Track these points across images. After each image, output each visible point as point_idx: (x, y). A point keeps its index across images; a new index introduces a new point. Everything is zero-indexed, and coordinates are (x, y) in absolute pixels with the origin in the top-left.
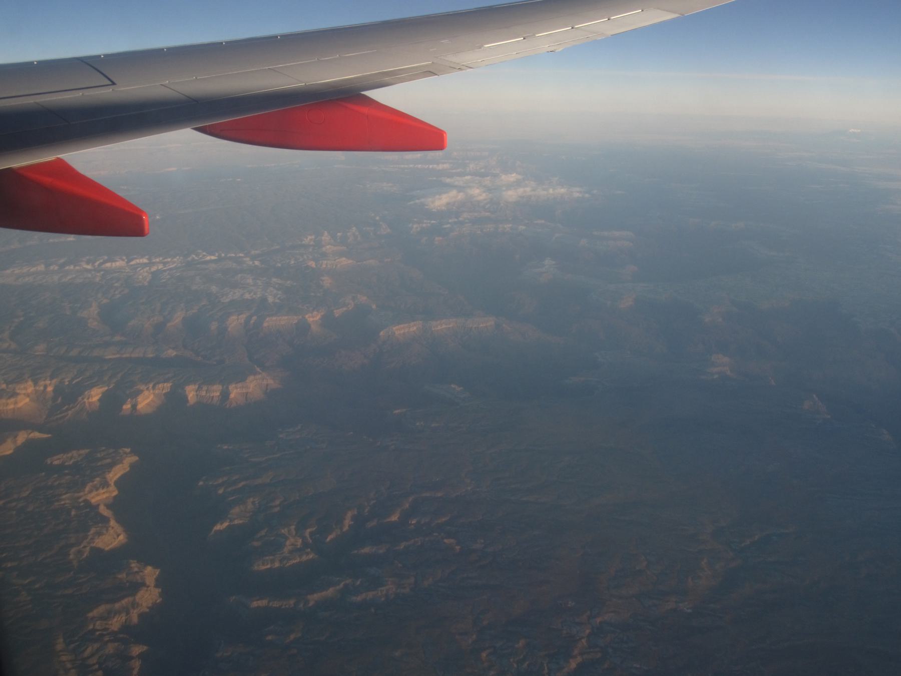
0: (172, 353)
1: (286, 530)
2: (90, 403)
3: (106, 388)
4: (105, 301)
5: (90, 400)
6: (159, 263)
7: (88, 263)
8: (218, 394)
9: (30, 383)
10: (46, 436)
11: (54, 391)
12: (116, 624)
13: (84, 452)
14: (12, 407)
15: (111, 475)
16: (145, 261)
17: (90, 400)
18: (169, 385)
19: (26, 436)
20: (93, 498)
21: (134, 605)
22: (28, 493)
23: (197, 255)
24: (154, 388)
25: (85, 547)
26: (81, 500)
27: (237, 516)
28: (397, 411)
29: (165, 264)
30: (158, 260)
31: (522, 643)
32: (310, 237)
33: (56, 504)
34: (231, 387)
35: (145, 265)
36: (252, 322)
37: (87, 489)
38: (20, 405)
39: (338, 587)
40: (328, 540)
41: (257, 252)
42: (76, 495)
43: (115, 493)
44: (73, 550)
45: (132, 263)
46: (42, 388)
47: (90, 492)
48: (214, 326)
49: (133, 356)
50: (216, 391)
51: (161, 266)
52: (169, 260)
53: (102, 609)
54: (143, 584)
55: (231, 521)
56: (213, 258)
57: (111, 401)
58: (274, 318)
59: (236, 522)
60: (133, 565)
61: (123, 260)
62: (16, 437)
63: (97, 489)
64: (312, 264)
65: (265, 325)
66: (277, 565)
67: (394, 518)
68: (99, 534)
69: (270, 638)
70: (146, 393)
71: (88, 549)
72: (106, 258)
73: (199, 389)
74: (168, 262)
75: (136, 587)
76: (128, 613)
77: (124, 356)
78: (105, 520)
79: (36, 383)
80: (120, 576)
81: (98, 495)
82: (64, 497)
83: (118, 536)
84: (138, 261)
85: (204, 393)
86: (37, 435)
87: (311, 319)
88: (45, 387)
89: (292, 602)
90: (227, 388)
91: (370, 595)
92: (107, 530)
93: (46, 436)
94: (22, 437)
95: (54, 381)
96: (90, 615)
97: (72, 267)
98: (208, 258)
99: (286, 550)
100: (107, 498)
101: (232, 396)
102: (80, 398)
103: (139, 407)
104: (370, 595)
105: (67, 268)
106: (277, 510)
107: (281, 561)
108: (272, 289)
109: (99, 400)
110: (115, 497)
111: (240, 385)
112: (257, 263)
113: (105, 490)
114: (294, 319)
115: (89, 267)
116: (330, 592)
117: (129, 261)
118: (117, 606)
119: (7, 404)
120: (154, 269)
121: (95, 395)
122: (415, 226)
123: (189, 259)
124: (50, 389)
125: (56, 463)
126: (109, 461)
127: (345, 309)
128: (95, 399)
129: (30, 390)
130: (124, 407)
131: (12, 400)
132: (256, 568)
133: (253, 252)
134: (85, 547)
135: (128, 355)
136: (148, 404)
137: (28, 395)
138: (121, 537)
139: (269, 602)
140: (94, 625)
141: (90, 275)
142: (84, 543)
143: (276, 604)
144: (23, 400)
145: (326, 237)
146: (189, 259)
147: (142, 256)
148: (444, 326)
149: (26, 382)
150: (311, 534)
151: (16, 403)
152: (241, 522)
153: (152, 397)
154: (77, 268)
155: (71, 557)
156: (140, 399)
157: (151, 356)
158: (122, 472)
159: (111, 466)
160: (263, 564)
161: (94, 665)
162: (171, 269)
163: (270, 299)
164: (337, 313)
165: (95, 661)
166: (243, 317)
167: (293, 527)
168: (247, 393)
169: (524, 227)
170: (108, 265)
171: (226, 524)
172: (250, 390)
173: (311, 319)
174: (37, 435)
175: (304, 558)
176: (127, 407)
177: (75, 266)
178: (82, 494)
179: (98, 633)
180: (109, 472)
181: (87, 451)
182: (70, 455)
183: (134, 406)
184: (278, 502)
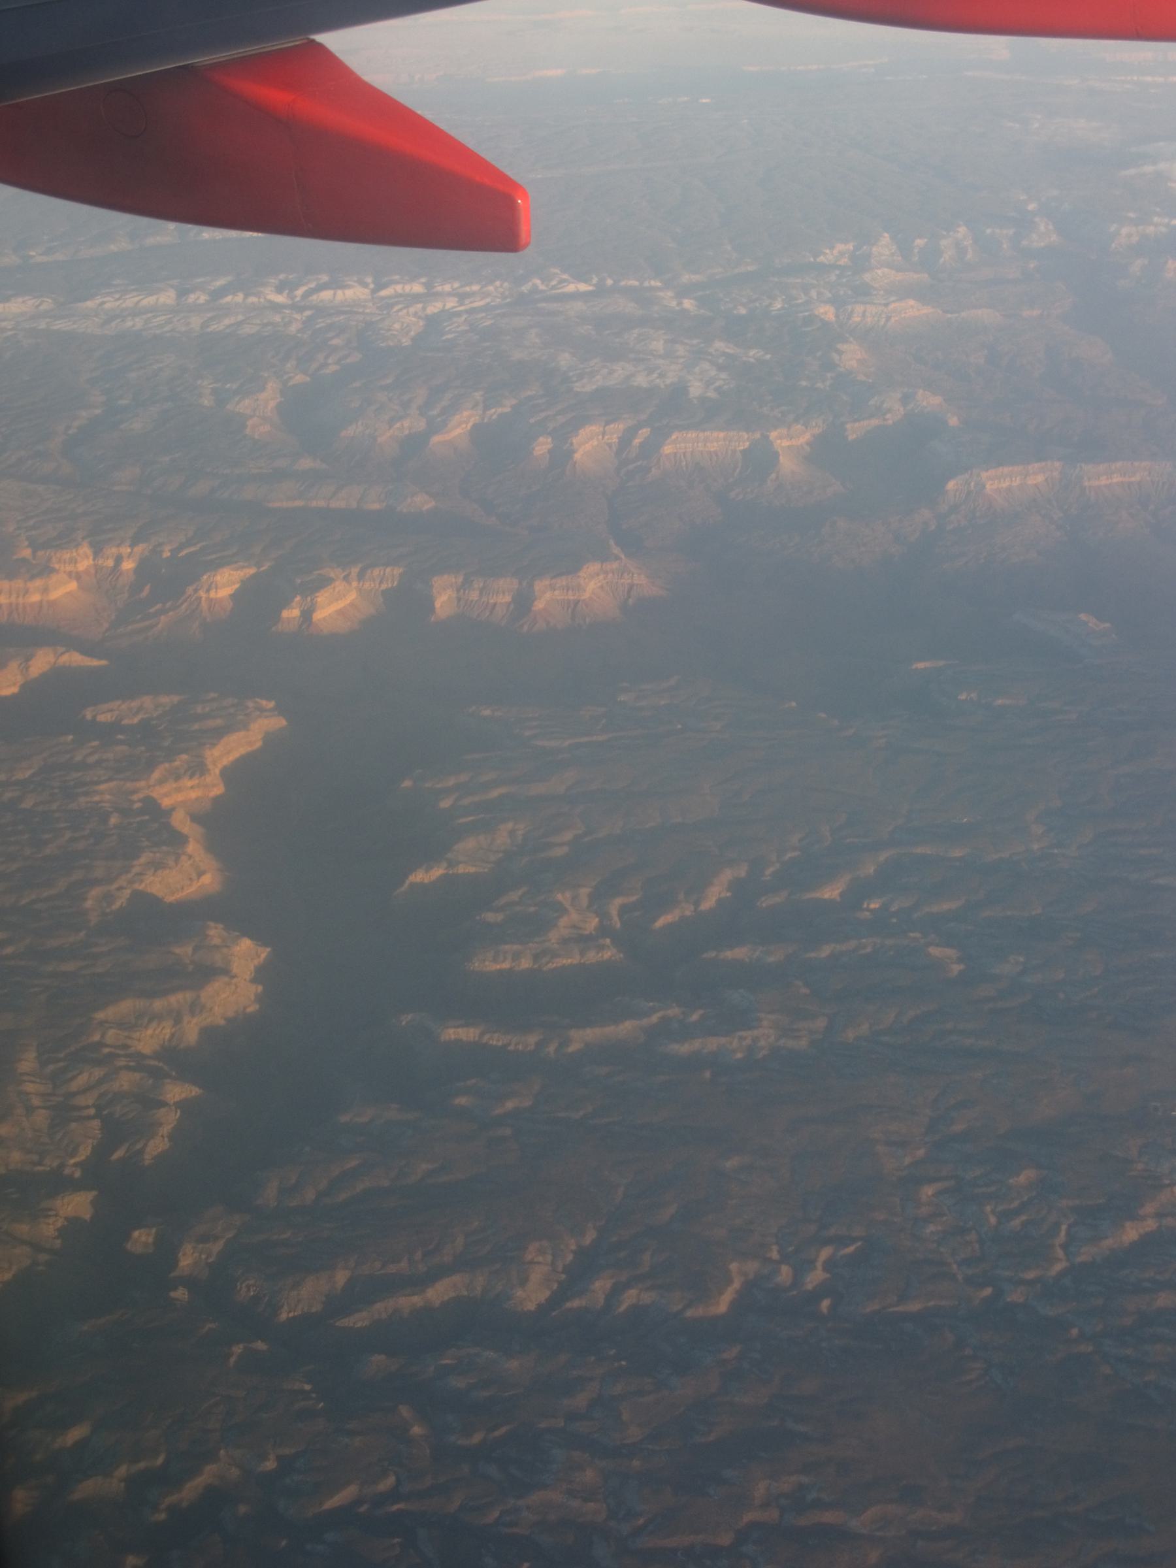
0: (422, 502)
1: (568, 894)
2: (210, 600)
3: (252, 571)
4: (299, 378)
5: (212, 595)
6: (449, 294)
7: (279, 290)
8: (508, 598)
9: (85, 549)
10: (95, 663)
11: (137, 571)
12: (148, 1040)
14: (35, 598)
15: (216, 752)
16: (417, 288)
17: (212, 595)
18: (398, 571)
19: (51, 658)
20: (166, 795)
21: (195, 1008)
22: (28, 773)
24: (361, 576)
25: (120, 888)
26: (135, 797)
27: (470, 857)
29: (462, 297)
30: (447, 288)
31: (1026, 1176)
32: (840, 247)
33: (82, 799)
34: (539, 585)
35: (416, 298)
37: (156, 775)
38: (54, 595)
39: (645, 1022)
40: (660, 923)
41: (696, 278)
42: (129, 785)
43: (219, 790)
44: (96, 892)
45: (383, 293)
46: (110, 563)
47: (161, 782)
49: (334, 504)
50: (502, 592)
51: (451, 303)
52: (475, 288)
53: (126, 1006)
54: (226, 971)
55: (451, 864)
56: (583, 287)
57: (259, 600)
58: (692, 435)
59: (461, 869)
60: (212, 932)
61: (365, 285)
62: (28, 659)
63: (178, 778)
64: (827, 312)
65: (667, 449)
66: (525, 964)
67: (831, 893)
68: (158, 866)
69: (462, 1101)
70: (340, 586)
71: (127, 893)
72: (325, 278)
74: (473, 294)
75: (206, 973)
76: (178, 1020)
77: (314, 504)
78: (179, 840)
79: (97, 552)
80: (177, 951)
81: (179, 790)
82: (102, 787)
83: (200, 874)
84: (399, 288)
85: (474, 595)
86: (75, 659)
87: (785, 443)
88: (119, 560)
89: (532, 1039)
91: (713, 1044)
92: (177, 861)
93: (95, 663)
94: (42, 661)
95: (139, 549)
96: (100, 1015)
97: (239, 298)
98: (571, 288)
99: (554, 936)
100: (197, 799)
101: (539, 605)
102: (190, 590)
103: (318, 616)
104: (713, 1044)
105: (229, 298)
106: (559, 852)
107: (536, 957)
108: (706, 365)
109: (233, 596)
110: (216, 800)
111: (562, 581)
112: (688, 304)
113: (195, 781)
114: (742, 441)
115: (280, 299)
116: (626, 1028)
117: (380, 286)
118: (158, 1004)
119: (27, 592)
120: (434, 308)
121: (224, 585)
122: (1124, 231)
123: (525, 289)
124: (128, 565)
125: (101, 718)
126: (219, 722)
127: (875, 422)
128: (224, 593)
129: (84, 564)
130: (285, 614)
131: (38, 583)
132: (476, 965)
133: (686, 278)
134: (120, 888)
135: (322, 504)
136: (341, 612)
137: (78, 577)
138: (207, 879)
139: (482, 1034)
140: (103, 1036)
141: (277, 318)
142: (122, 881)
143: (496, 1040)
144: (64, 585)
145: (884, 247)
146: (525, 289)
147: (413, 278)
148: (1116, 479)
149: (77, 546)
150: (623, 910)
151: (46, 590)
152: (472, 870)
153: (352, 596)
154: (252, 299)
155: (89, 904)
156: (321, 597)
158: (242, 751)
159: (219, 733)
160: (495, 960)
161: (88, 1107)
162: (471, 311)
163: (696, 390)
164: (854, 430)
165: (90, 1102)
167: (584, 892)
168: (577, 602)
170: (326, 295)
171: (438, 872)
172: (586, 596)
173: (785, 443)
174: (75, 659)
175: (592, 957)
176: (292, 613)
177: (246, 296)
178: (143, 783)
179: (106, 1050)
180: (213, 745)
181: (176, 699)
182: (135, 704)
183: (307, 615)
184: (568, 836)
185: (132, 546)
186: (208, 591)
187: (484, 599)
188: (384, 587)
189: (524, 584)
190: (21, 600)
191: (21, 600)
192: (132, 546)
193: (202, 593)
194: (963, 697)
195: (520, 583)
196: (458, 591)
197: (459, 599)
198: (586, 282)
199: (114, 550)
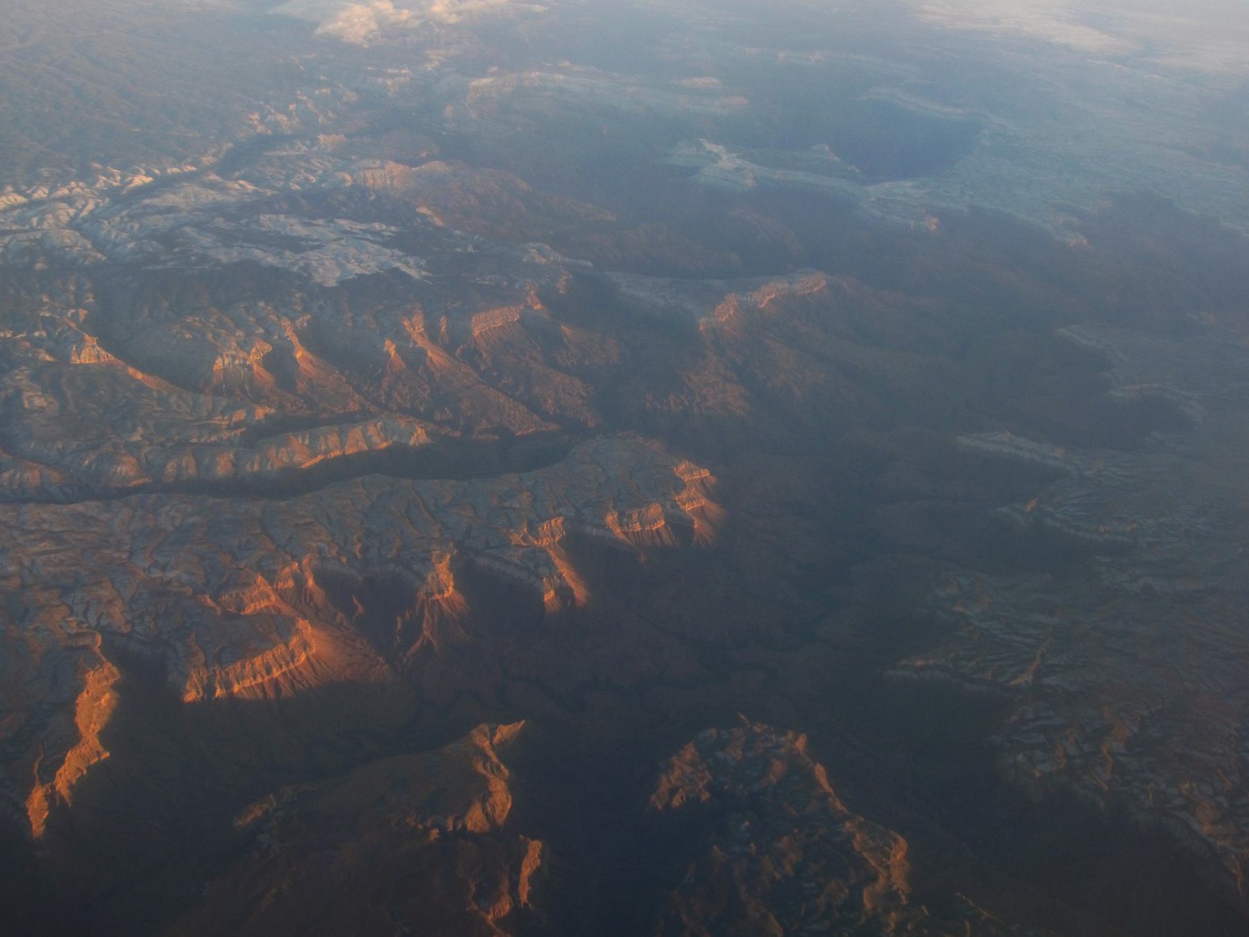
13: (689, 752)
23: (110, 176)
28: (1028, 508)
36: (443, 329)
48: (390, 348)
58: (483, 316)
65: (476, 332)
77: (333, 455)
90: (675, 506)
102: (421, 594)
111: (684, 495)
121: (442, 581)
126: (778, 767)
130: (546, 599)
135: (338, 453)
157: (385, 445)
169: (562, 77)
174: (505, 731)
176: (549, 596)
178: (882, 880)
183: (564, 593)
186: (441, 592)
188: (557, 538)
189: (668, 504)
190: (292, 666)
191: (292, 666)
193: (438, 596)
194: (1102, 529)
195: (663, 506)
196: (621, 526)
197: (626, 533)
198: (136, 173)
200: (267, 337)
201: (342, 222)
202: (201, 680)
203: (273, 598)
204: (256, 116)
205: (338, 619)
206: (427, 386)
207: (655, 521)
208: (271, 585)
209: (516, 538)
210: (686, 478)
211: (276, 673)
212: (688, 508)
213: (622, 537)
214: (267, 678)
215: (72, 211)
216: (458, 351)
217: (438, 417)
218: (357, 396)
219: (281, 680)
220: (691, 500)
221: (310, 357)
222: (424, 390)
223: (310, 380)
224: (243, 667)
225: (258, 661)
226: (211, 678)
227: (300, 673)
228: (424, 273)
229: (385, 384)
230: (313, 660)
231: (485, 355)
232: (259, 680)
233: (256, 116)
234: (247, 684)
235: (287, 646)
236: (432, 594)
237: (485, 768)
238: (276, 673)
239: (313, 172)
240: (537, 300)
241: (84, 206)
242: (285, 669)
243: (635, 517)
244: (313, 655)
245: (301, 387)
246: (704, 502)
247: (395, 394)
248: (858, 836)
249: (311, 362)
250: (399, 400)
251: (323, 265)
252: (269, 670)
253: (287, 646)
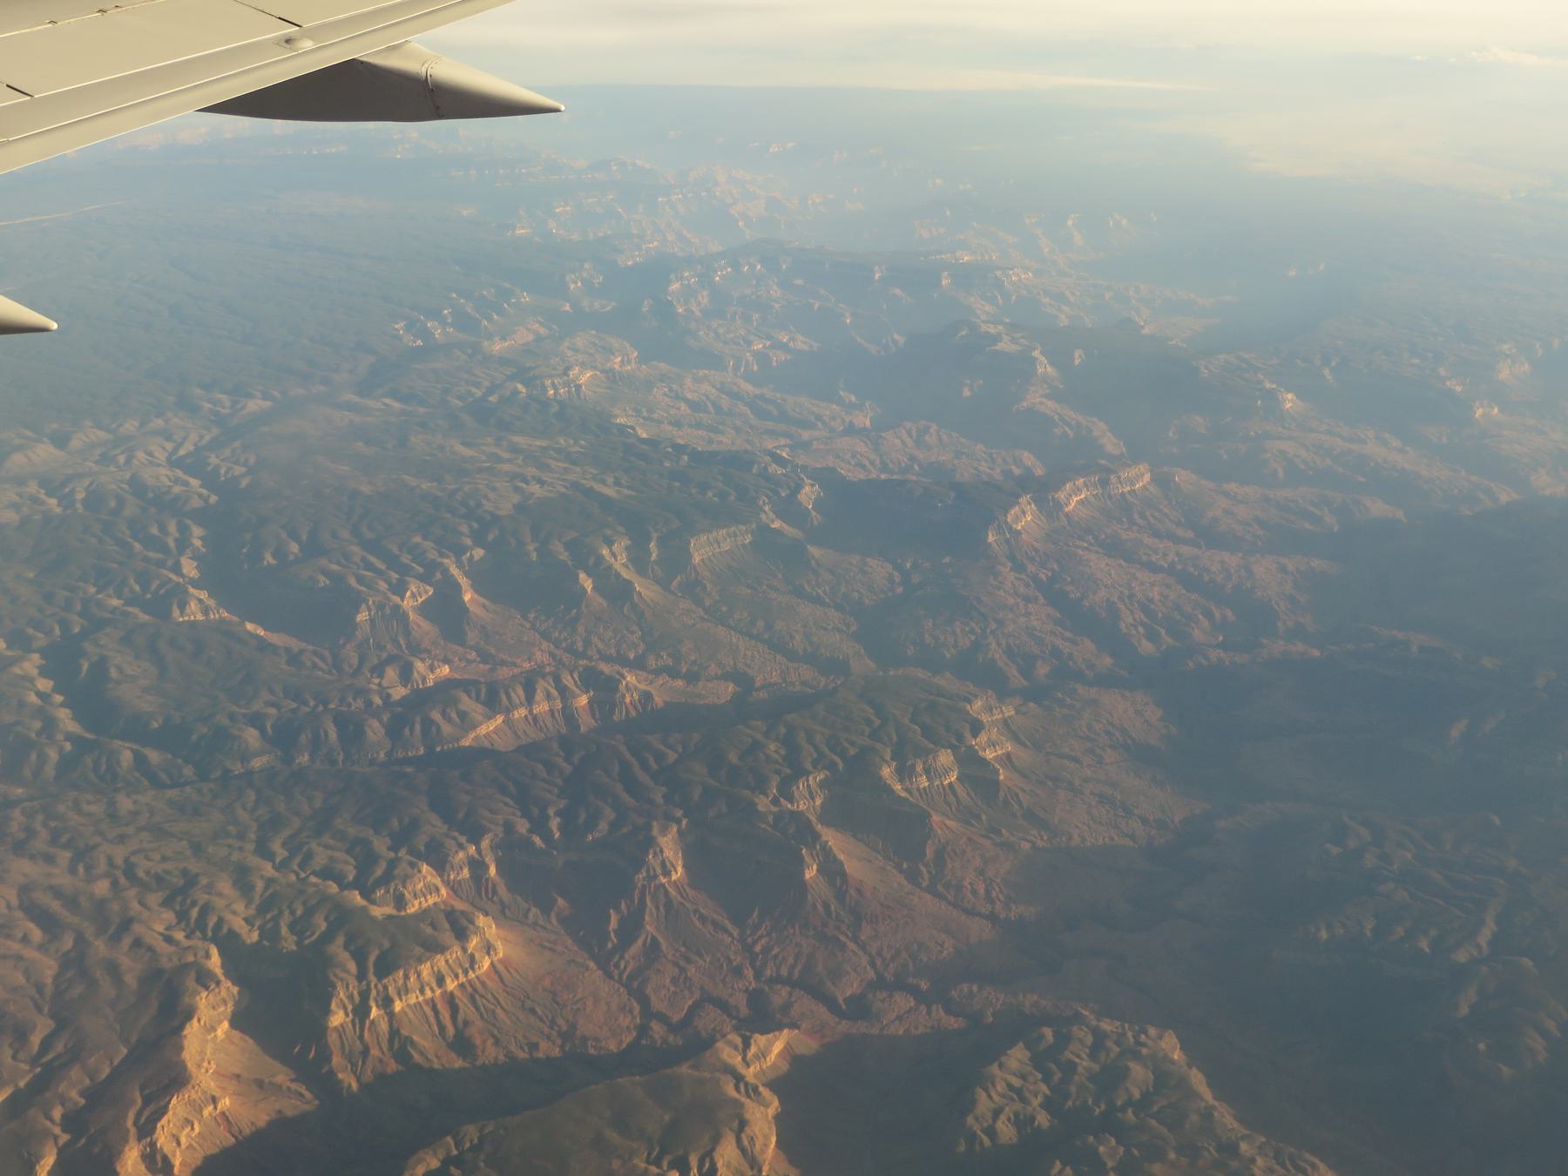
5: (674, 878)
17: (674, 878)
46: (466, 873)
58: (703, 538)
65: (697, 559)
73: (904, 773)
79: (440, 866)
85: (924, 782)
88: (477, 866)
95: (485, 843)
111: (983, 738)
130: (807, 876)
166: (621, 545)
185: (475, 839)
186: (667, 873)
187: (937, 783)
190: (472, 975)
192: (475, 839)
196: (901, 781)
199: (461, 855)
200: (425, 579)
201: (516, 439)
202: (351, 997)
203: (443, 891)
204: (400, 326)
205: (531, 916)
206: (635, 628)
207: (946, 772)
208: (441, 876)
209: (763, 803)
210: (985, 718)
211: (451, 985)
212: (989, 755)
213: (903, 794)
214: (438, 992)
215: (169, 446)
216: (675, 583)
217: (652, 662)
218: (545, 645)
219: (457, 993)
220: (993, 744)
221: (482, 600)
222: (632, 633)
223: (483, 627)
224: (406, 977)
225: (425, 970)
226: (365, 996)
227: (483, 984)
228: (626, 491)
229: (581, 629)
230: (500, 967)
231: (709, 586)
232: (429, 994)
233: (400, 326)
234: (413, 1001)
235: (464, 950)
236: (656, 877)
237: (737, 1089)
238: (451, 985)
239: (477, 385)
240: (772, 515)
241: (185, 439)
242: (462, 979)
243: (919, 768)
244: (500, 961)
245: (472, 636)
246: (1009, 747)
247: (595, 640)
248: (1260, 1161)
249: (484, 606)
250: (601, 646)
251: (494, 489)
252: (440, 981)
253: (464, 950)
